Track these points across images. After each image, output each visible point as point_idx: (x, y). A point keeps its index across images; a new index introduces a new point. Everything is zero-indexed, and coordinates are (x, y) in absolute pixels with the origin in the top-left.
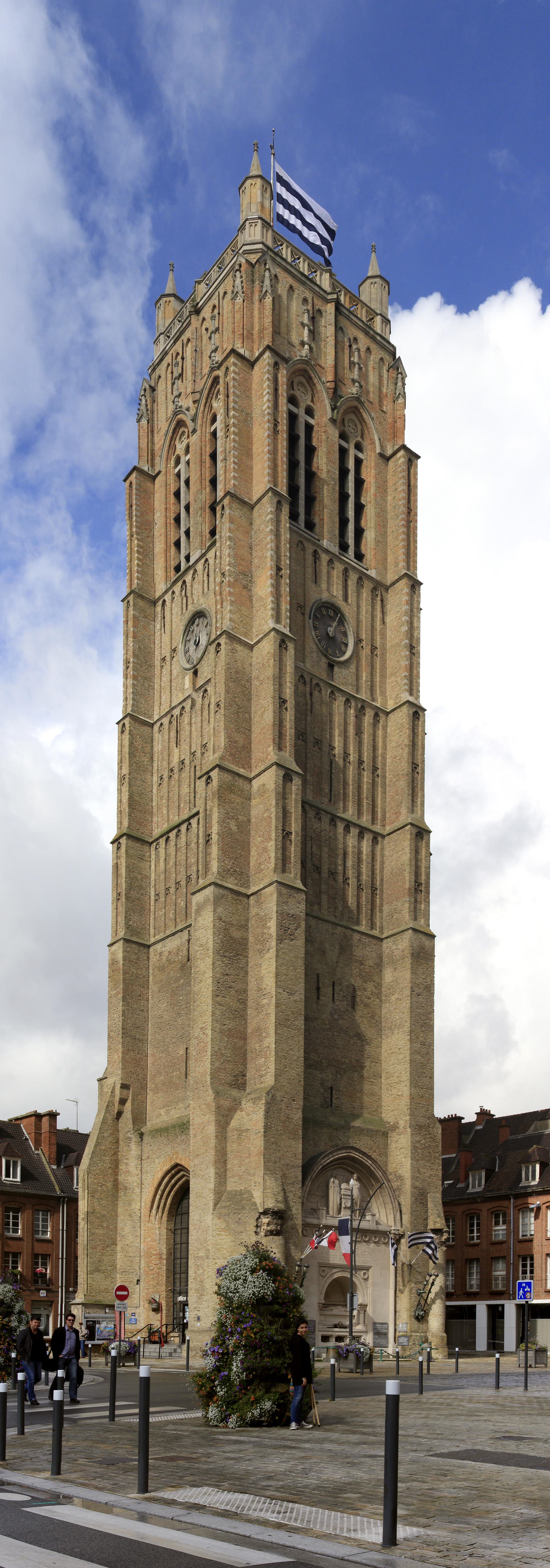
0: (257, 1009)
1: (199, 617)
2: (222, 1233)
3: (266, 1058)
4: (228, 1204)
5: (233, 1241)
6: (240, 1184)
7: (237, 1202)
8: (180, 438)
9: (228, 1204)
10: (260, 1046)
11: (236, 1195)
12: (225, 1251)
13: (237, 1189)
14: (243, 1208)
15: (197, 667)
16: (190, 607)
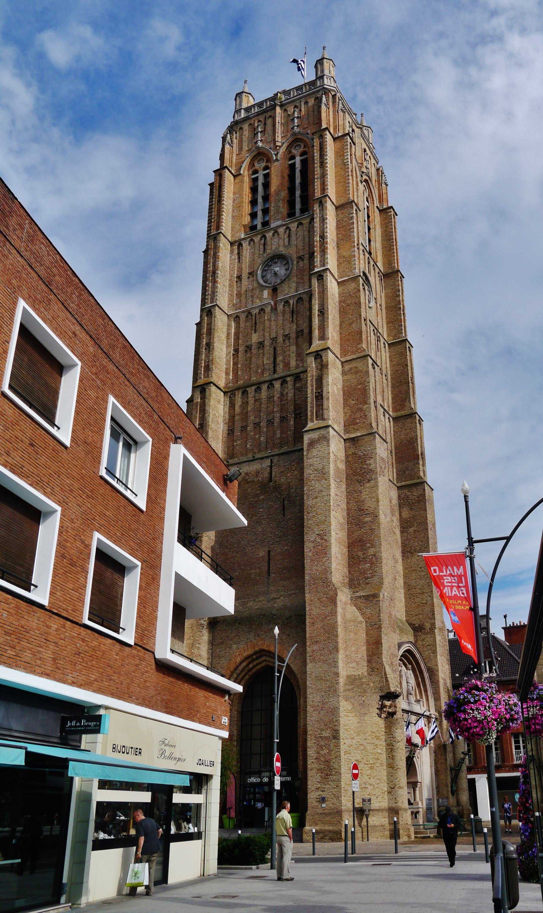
0: (358, 525)
1: (278, 258)
2: (349, 714)
3: (371, 564)
4: (351, 687)
5: (358, 722)
6: (358, 669)
7: (358, 686)
8: (258, 161)
9: (351, 687)
10: (364, 554)
11: (355, 679)
12: (352, 732)
13: (355, 673)
14: (365, 691)
15: (277, 287)
16: (268, 251)
